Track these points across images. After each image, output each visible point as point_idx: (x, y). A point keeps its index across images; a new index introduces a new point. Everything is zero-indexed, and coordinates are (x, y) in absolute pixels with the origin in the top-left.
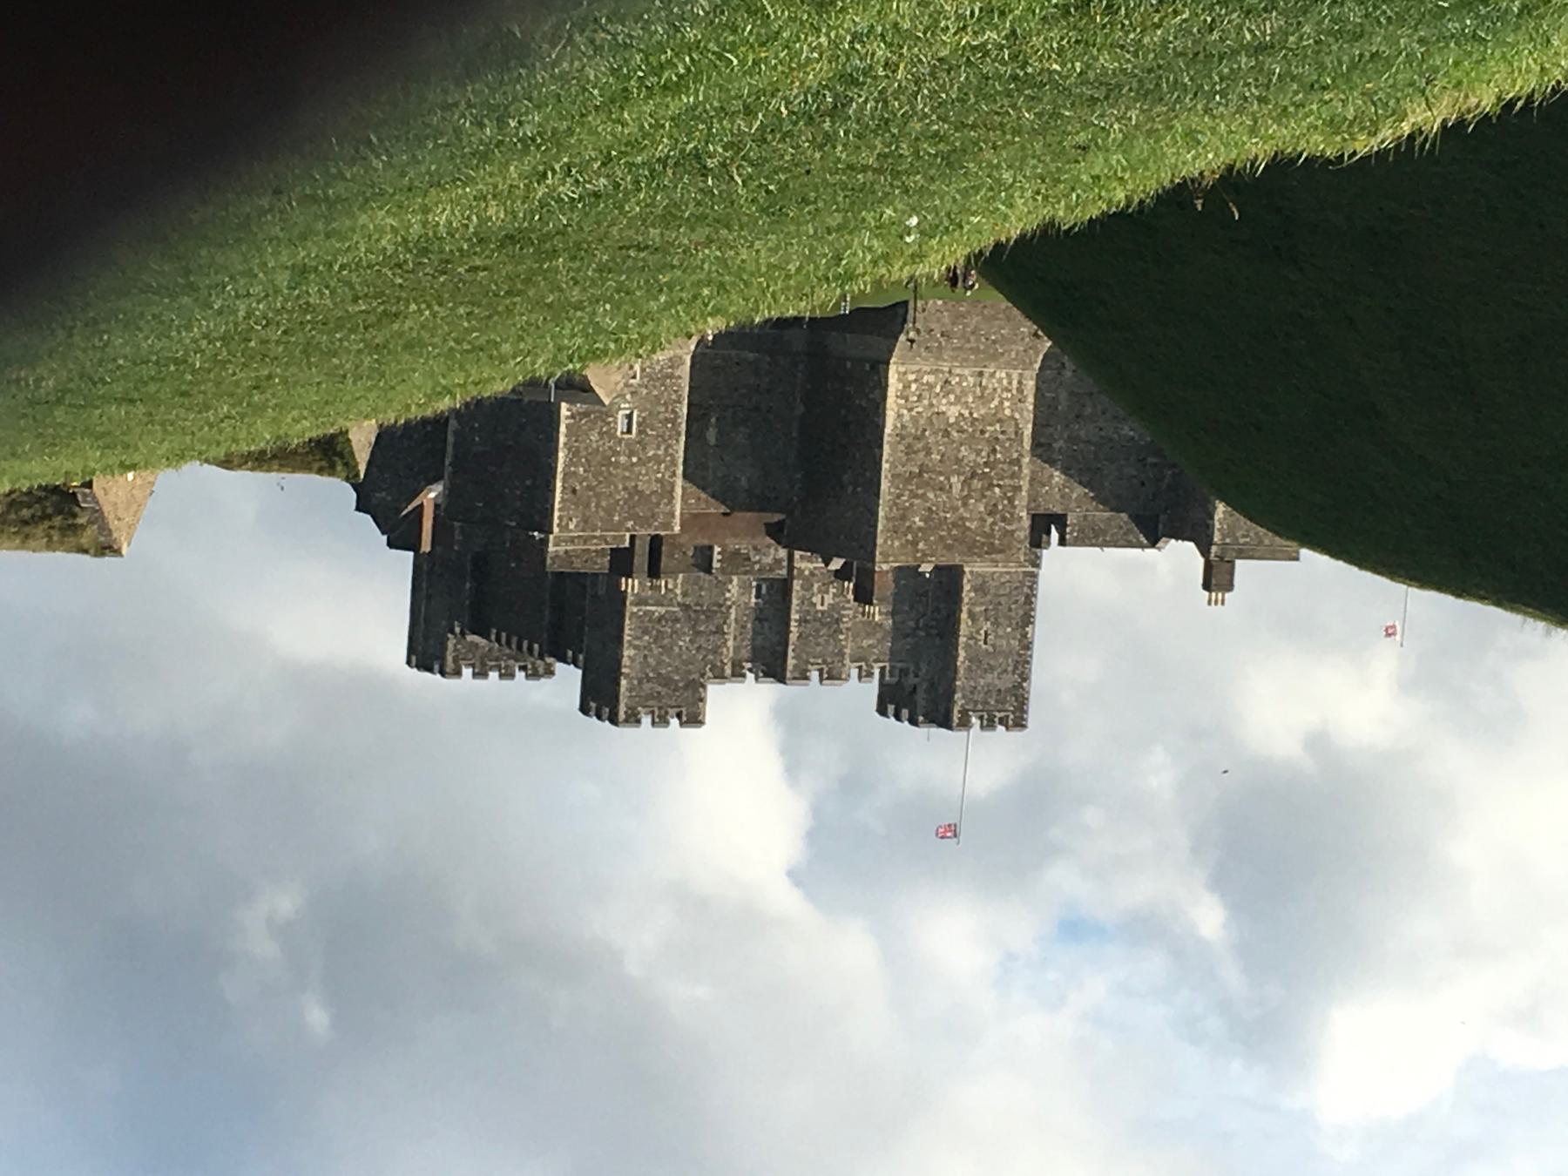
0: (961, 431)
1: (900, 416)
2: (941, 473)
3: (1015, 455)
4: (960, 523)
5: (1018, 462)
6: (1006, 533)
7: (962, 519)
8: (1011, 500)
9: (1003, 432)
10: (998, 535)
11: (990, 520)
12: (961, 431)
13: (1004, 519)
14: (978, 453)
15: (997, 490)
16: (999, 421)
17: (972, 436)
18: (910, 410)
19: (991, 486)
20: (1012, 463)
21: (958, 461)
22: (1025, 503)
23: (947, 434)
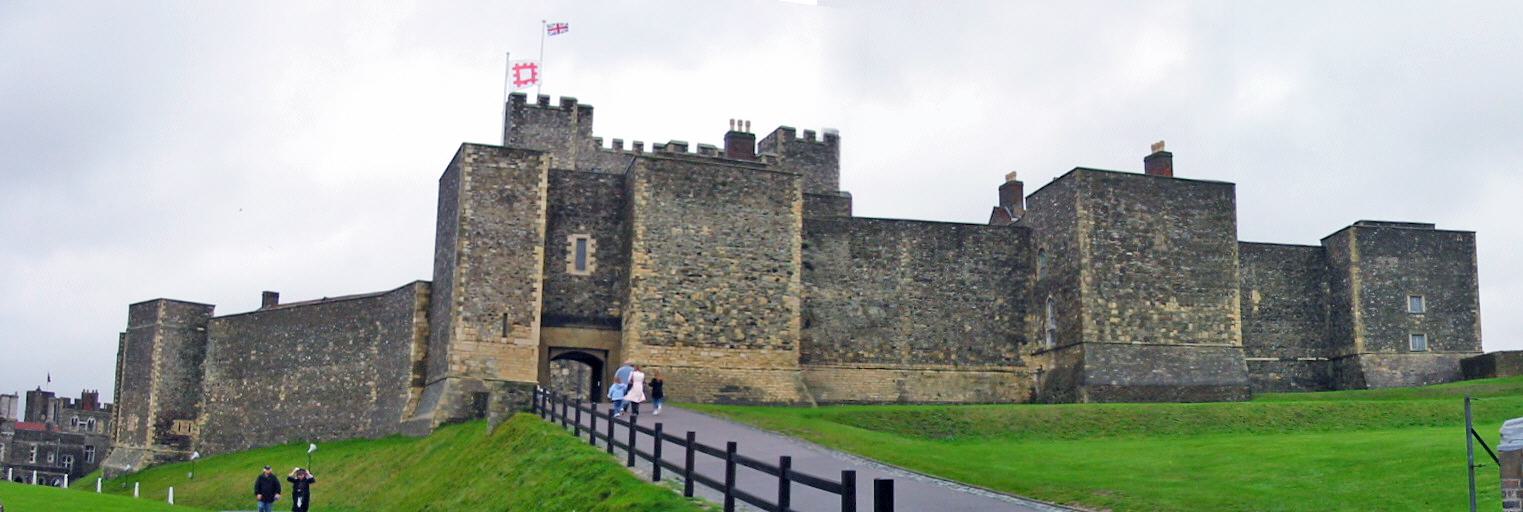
0: (1162, 289)
1: (1230, 304)
2: (1178, 254)
3: (1099, 265)
4: (1153, 208)
5: (1095, 259)
6: (1102, 195)
7: (1149, 212)
8: (1097, 227)
9: (1114, 286)
10: (1111, 195)
11: (1121, 209)
12: (1162, 289)
13: (1105, 209)
14: (1139, 270)
15: (1116, 236)
16: (1119, 297)
17: (1150, 285)
18: (1223, 308)
19: (1122, 240)
20: (1102, 259)
21: (1163, 263)
22: (1082, 222)
23: (1177, 287)
